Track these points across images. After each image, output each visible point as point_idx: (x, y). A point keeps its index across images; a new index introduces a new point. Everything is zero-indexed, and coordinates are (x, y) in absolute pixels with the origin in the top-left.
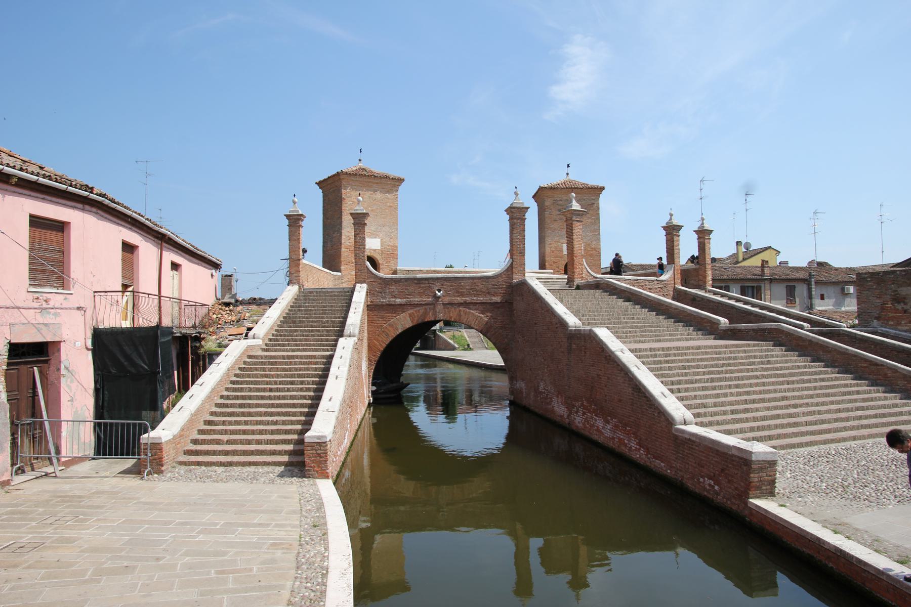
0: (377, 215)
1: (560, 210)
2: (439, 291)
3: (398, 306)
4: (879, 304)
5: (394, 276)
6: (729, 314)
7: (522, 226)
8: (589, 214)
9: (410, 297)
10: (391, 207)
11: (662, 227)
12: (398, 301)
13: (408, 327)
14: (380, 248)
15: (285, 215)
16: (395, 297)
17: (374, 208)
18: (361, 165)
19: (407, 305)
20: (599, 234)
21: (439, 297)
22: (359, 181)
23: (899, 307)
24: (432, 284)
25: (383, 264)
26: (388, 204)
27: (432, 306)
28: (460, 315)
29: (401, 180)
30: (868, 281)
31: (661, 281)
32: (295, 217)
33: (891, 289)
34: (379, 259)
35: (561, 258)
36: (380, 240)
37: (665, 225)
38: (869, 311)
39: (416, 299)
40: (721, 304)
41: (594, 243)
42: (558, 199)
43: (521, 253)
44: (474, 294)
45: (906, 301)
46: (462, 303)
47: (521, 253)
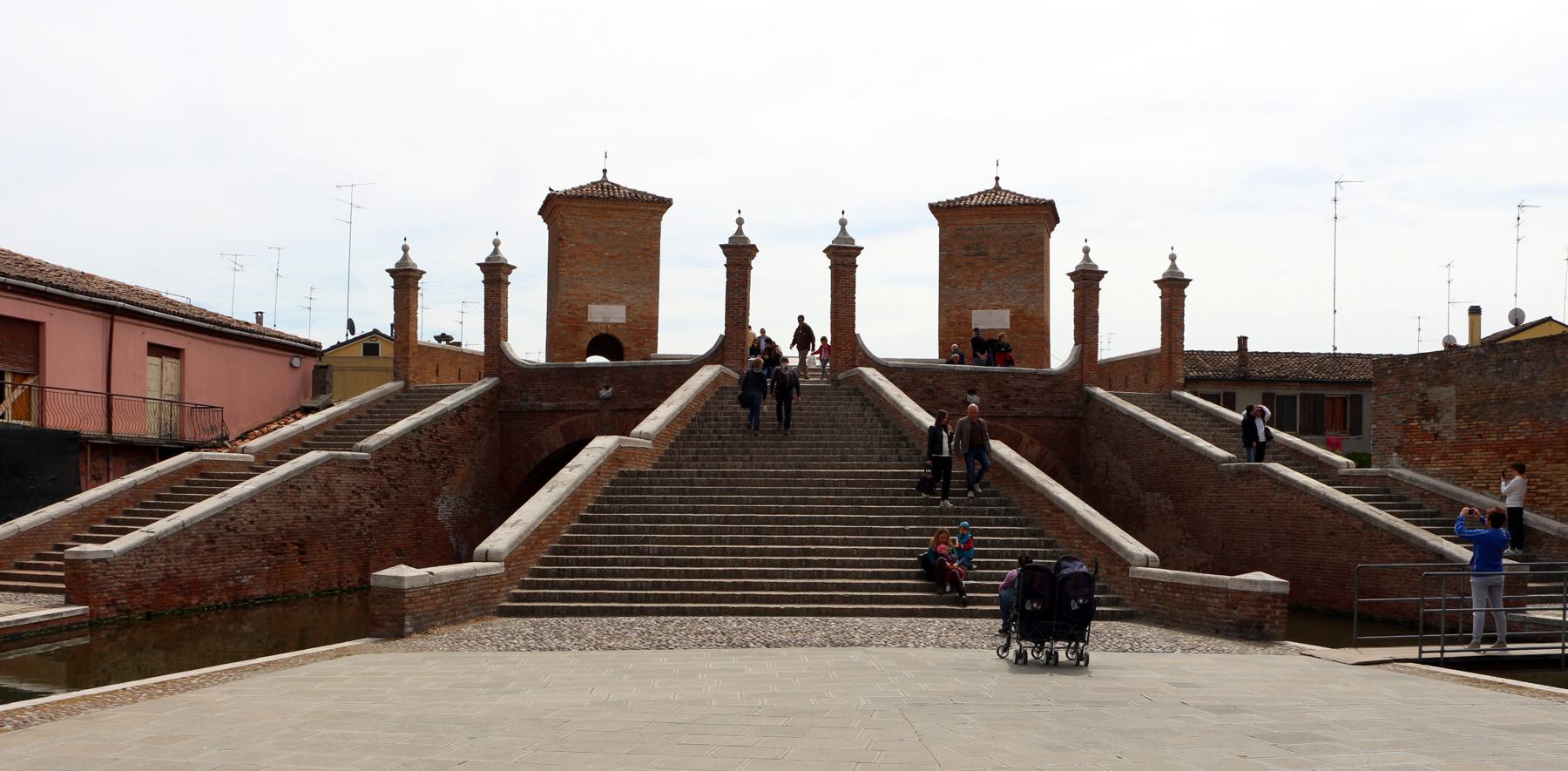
0: (618, 265)
1: (968, 248)
2: (607, 388)
6: (1139, 437)
7: (742, 277)
8: (1022, 253)
9: (562, 398)
10: (648, 249)
11: (1068, 274)
12: (546, 405)
13: (558, 447)
14: (624, 322)
15: (387, 271)
16: (540, 399)
19: (558, 411)
22: (588, 207)
24: (597, 377)
25: (630, 348)
26: (642, 245)
29: (665, 203)
32: (403, 273)
33: (1418, 391)
34: (622, 340)
36: (624, 308)
37: (1073, 270)
38: (1387, 435)
39: (572, 403)
40: (1133, 419)
41: (1032, 307)
42: (966, 228)
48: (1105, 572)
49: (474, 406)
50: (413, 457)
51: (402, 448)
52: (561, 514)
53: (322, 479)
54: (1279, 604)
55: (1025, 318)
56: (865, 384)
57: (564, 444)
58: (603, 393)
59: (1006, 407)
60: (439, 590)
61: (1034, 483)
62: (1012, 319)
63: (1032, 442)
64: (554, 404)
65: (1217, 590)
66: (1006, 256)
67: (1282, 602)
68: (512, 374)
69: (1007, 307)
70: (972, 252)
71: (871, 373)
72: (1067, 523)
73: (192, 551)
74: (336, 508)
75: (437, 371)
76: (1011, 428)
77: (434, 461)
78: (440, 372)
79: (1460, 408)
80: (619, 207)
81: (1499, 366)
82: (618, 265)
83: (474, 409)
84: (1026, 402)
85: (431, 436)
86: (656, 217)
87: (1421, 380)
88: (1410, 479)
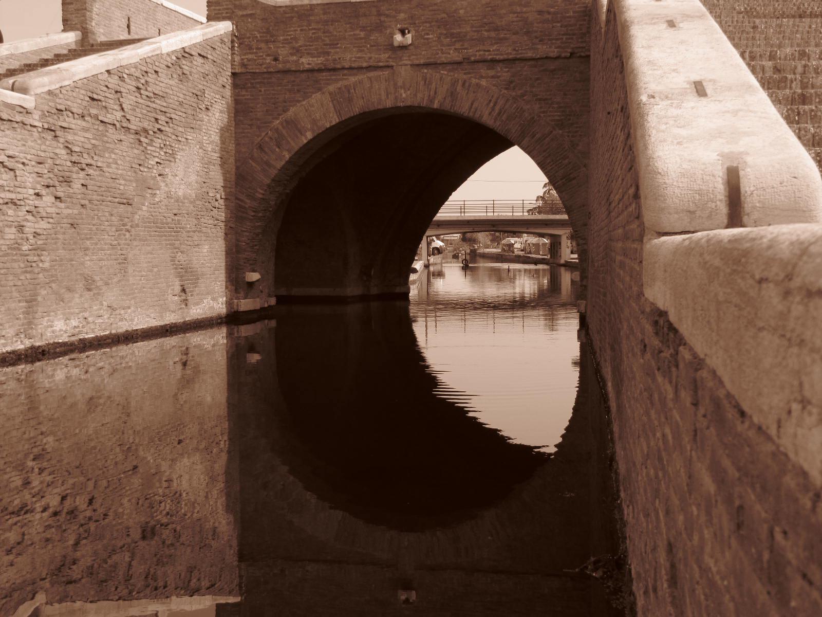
2: (403, 33)
3: (304, 76)
12: (306, 62)
13: (328, 126)
16: (297, 51)
21: (403, 47)
24: (387, 16)
27: (386, 72)
28: (453, 94)
39: (348, 56)
44: (489, 38)
46: (459, 63)
49: (200, 55)
50: (109, 118)
51: (93, 99)
57: (335, 120)
64: (321, 60)
68: (251, 15)
75: (128, 26)
78: (132, 28)
83: (200, 60)
85: (138, 88)
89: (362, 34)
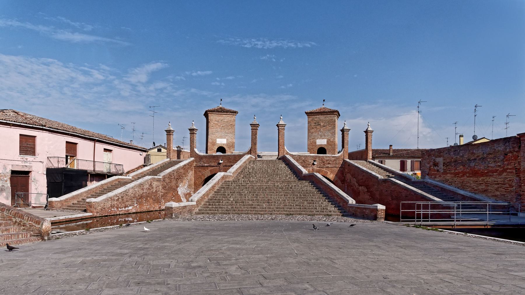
1: (315, 123)
2: (222, 160)
4: (428, 167)
5: (233, 154)
10: (232, 125)
11: (340, 130)
17: (224, 125)
18: (221, 106)
20: (335, 134)
23: (436, 168)
26: (231, 124)
30: (425, 155)
31: (335, 157)
35: (315, 146)
36: (226, 140)
39: (213, 164)
41: (332, 138)
43: (255, 144)
45: (438, 165)
47: (255, 144)
48: (342, 205)
52: (210, 191)
53: (150, 183)
54: (383, 212)
55: (330, 141)
56: (286, 159)
58: (221, 162)
59: (324, 165)
60: (181, 208)
61: (326, 183)
62: (327, 142)
63: (330, 174)
65: (368, 209)
66: (325, 125)
67: (383, 211)
69: (326, 139)
70: (316, 124)
71: (288, 156)
72: (333, 193)
73: (118, 200)
74: (153, 190)
76: (325, 170)
77: (178, 178)
79: (444, 163)
80: (224, 114)
81: (454, 152)
82: (225, 129)
83: (188, 166)
84: (329, 163)
86: (234, 116)
87: (434, 156)
88: (431, 182)
89: (215, 160)
